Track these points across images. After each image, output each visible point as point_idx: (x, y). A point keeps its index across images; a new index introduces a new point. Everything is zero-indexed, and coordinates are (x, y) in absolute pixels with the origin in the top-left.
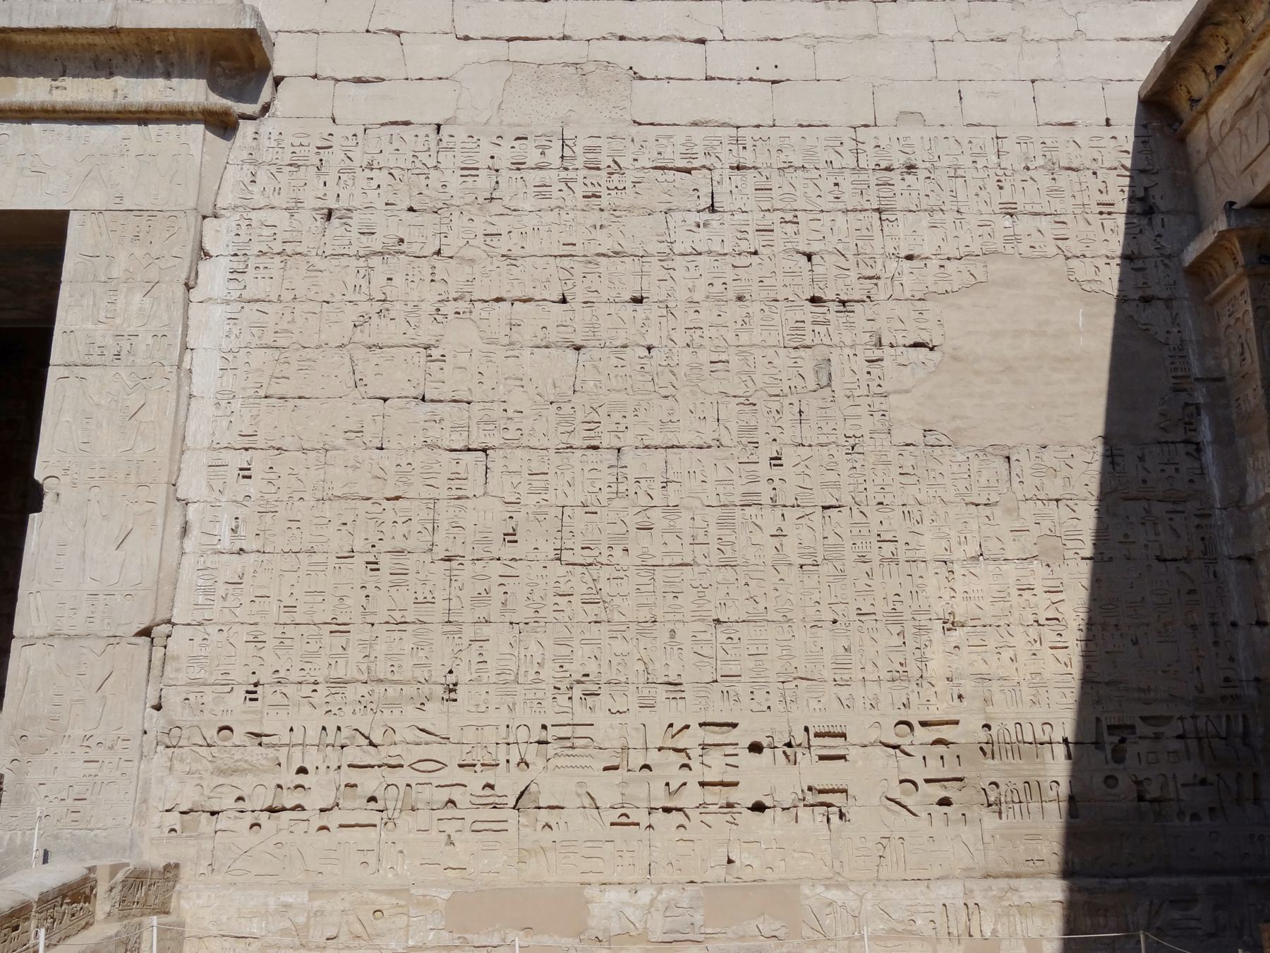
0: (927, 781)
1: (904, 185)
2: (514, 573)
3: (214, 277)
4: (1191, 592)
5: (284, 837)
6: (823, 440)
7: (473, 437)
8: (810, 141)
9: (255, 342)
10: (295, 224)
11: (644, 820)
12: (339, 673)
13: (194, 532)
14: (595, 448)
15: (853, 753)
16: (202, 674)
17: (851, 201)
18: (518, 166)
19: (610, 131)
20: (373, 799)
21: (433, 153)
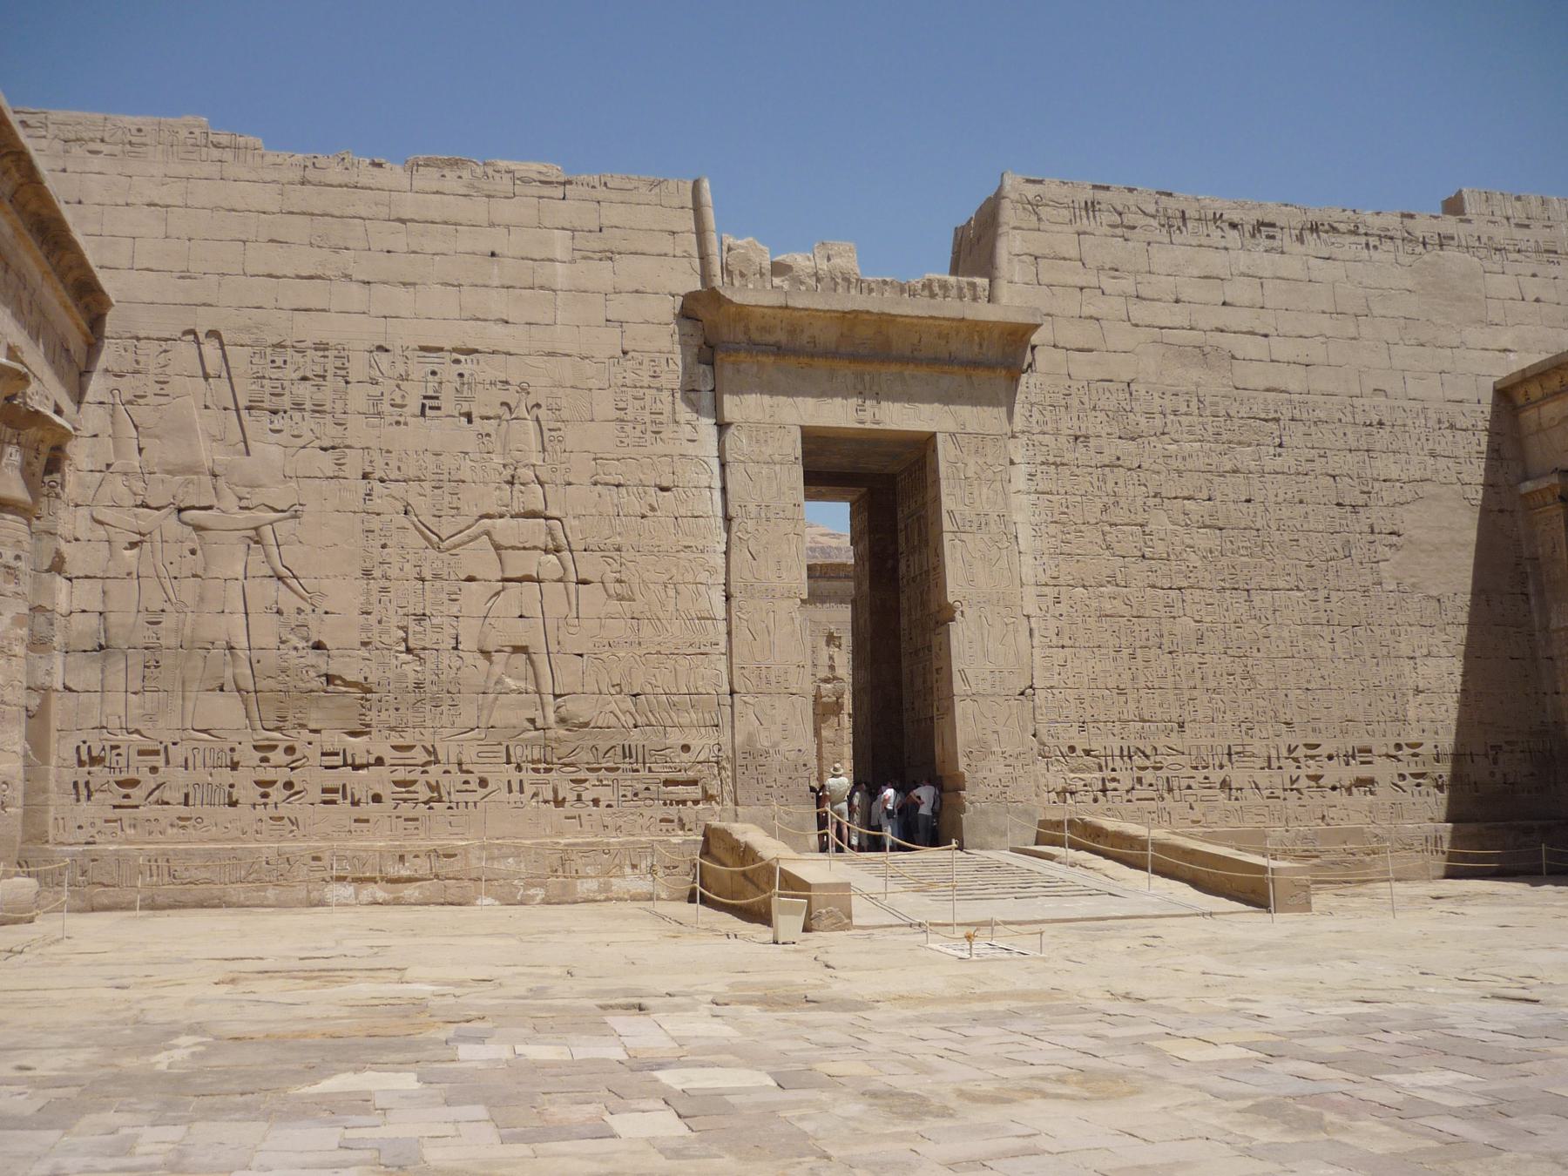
0: (1412, 775)
1: (1379, 436)
2: (1204, 661)
3: (1019, 475)
4: (1526, 676)
5: (1110, 805)
6: (1350, 587)
7: (1174, 580)
8: (1329, 406)
9: (1050, 519)
10: (1059, 445)
11: (1282, 797)
12: (1125, 717)
13: (1036, 633)
14: (1236, 589)
15: (1376, 760)
16: (1055, 717)
17: (1354, 445)
18: (1175, 413)
19: (1223, 391)
20: (1151, 785)
21: (1128, 401)
